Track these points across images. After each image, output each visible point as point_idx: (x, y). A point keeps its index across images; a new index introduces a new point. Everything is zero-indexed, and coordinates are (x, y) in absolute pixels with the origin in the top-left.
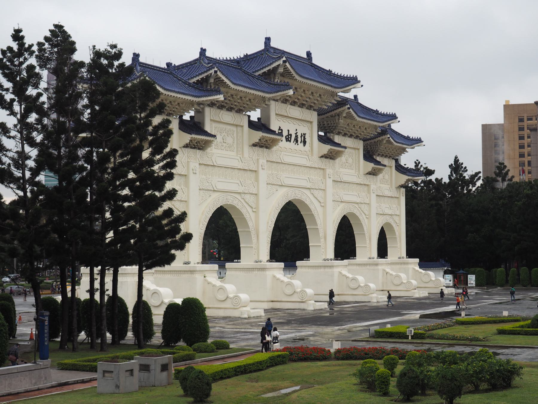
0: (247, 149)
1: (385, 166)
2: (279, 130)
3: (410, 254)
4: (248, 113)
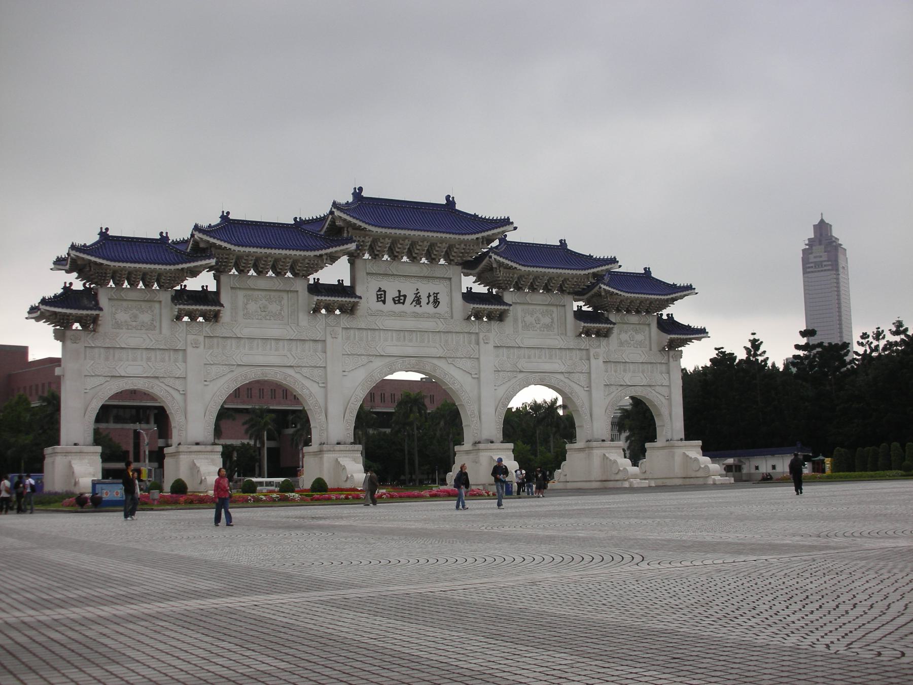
0: (304, 319)
1: (614, 324)
2: (380, 290)
3: (690, 434)
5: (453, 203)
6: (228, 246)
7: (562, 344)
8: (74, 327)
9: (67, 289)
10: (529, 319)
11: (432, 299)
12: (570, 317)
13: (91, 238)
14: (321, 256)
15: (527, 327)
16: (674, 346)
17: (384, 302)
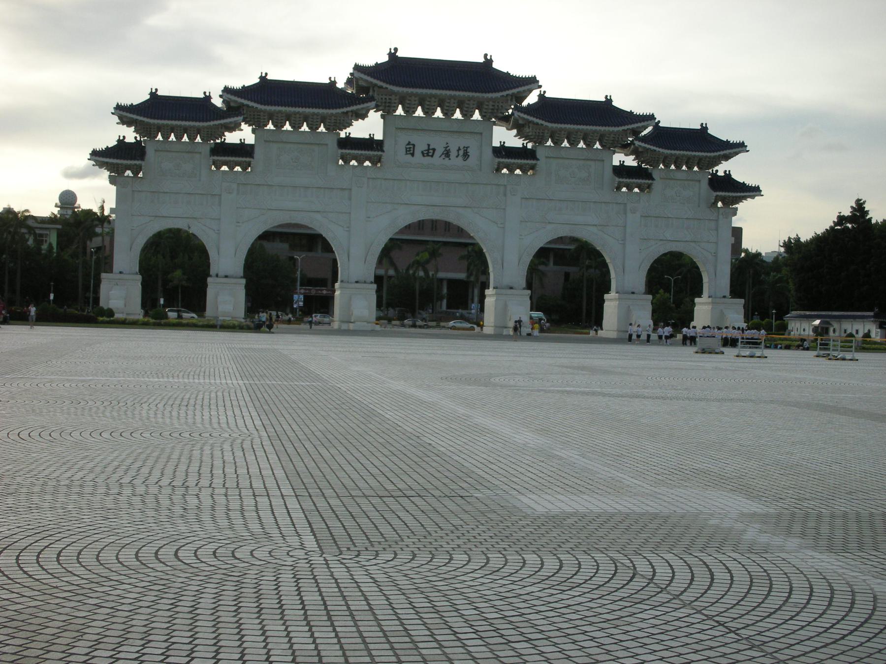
2: (409, 143)
4: (344, 131)
6: (255, 105)
8: (126, 174)
9: (121, 142)
11: (461, 152)
12: (609, 172)
13: (140, 96)
14: (347, 112)
16: (731, 203)
17: (413, 155)
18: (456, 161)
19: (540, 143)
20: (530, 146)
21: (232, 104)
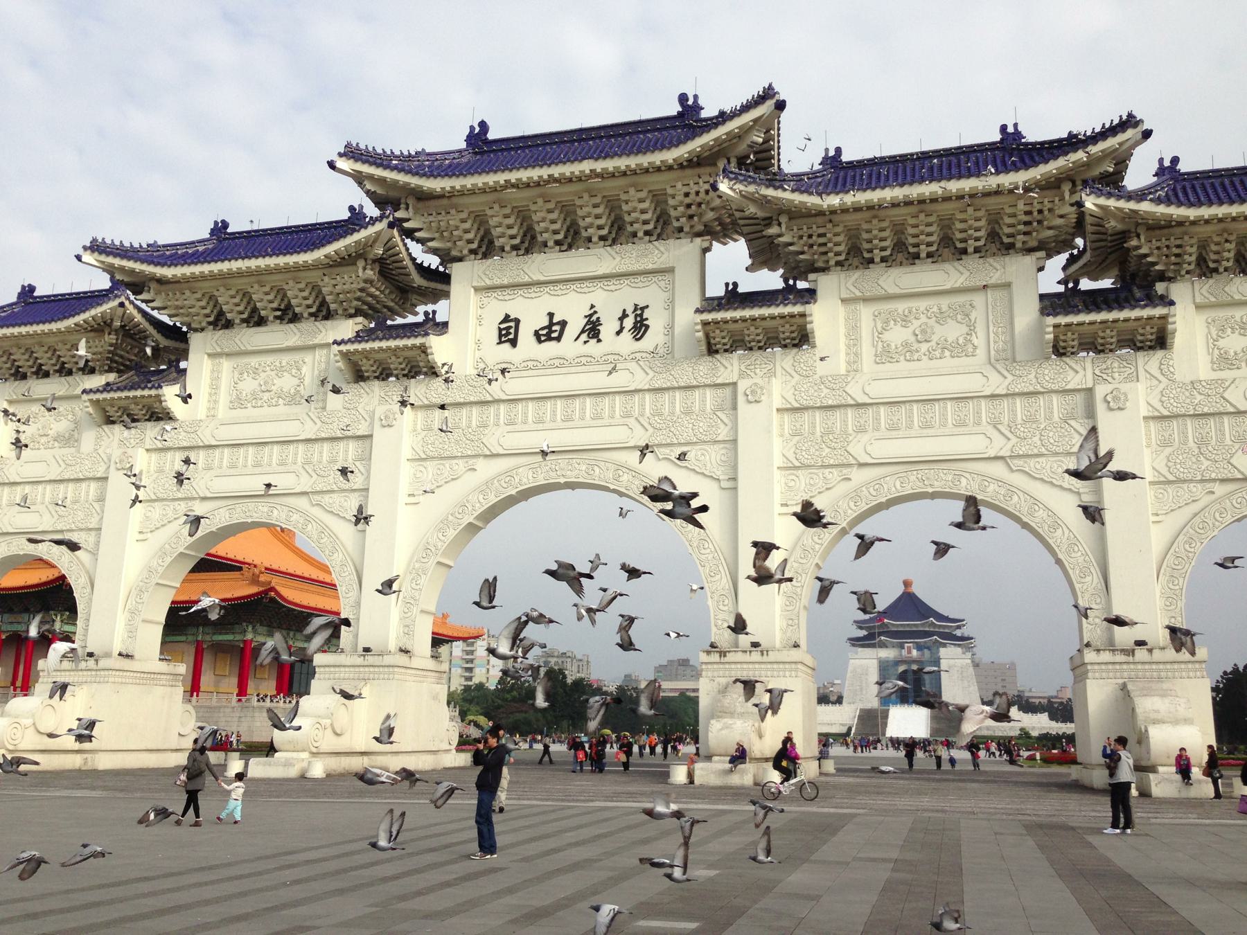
1: (1172, 303)
2: (507, 319)
5: (697, 108)
7: (997, 383)
10: (897, 335)
11: (629, 323)
15: (885, 355)
17: (514, 343)
18: (613, 341)
19: (824, 270)
20: (801, 285)
21: (118, 277)
